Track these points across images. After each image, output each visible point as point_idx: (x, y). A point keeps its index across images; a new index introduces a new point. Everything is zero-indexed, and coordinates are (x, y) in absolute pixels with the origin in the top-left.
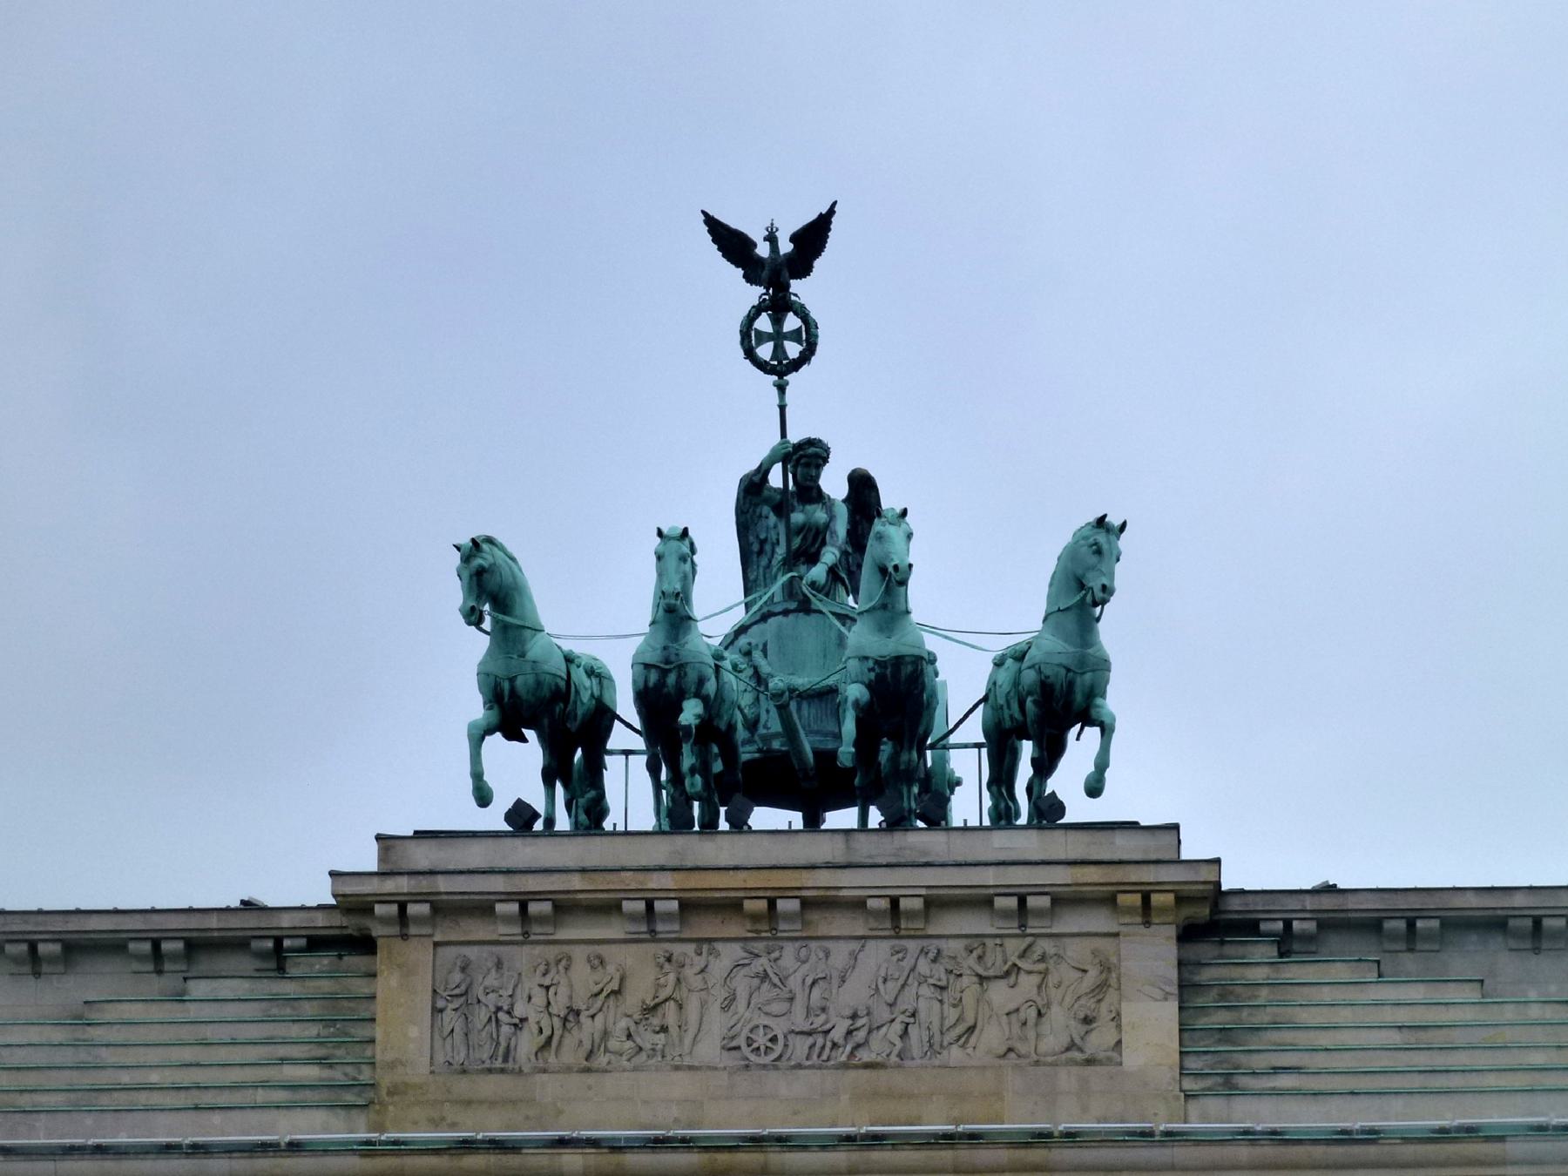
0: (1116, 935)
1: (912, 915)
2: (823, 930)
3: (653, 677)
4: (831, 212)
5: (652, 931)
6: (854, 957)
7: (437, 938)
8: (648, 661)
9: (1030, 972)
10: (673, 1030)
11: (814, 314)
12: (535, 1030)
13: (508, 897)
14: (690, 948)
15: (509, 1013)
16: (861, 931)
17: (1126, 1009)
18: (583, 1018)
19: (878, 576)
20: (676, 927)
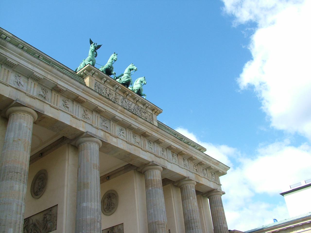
0: (152, 114)
1: (139, 102)
2: (130, 100)
3: (110, 67)
4: (101, 45)
5: (116, 91)
6: (132, 104)
7: (95, 79)
8: (109, 65)
9: (147, 113)
10: (118, 102)
11: (97, 53)
12: (105, 94)
13: (106, 78)
14: (118, 95)
15: (102, 91)
16: (133, 102)
17: (154, 121)
18: (110, 96)
19: (129, 71)
20: (118, 91)
